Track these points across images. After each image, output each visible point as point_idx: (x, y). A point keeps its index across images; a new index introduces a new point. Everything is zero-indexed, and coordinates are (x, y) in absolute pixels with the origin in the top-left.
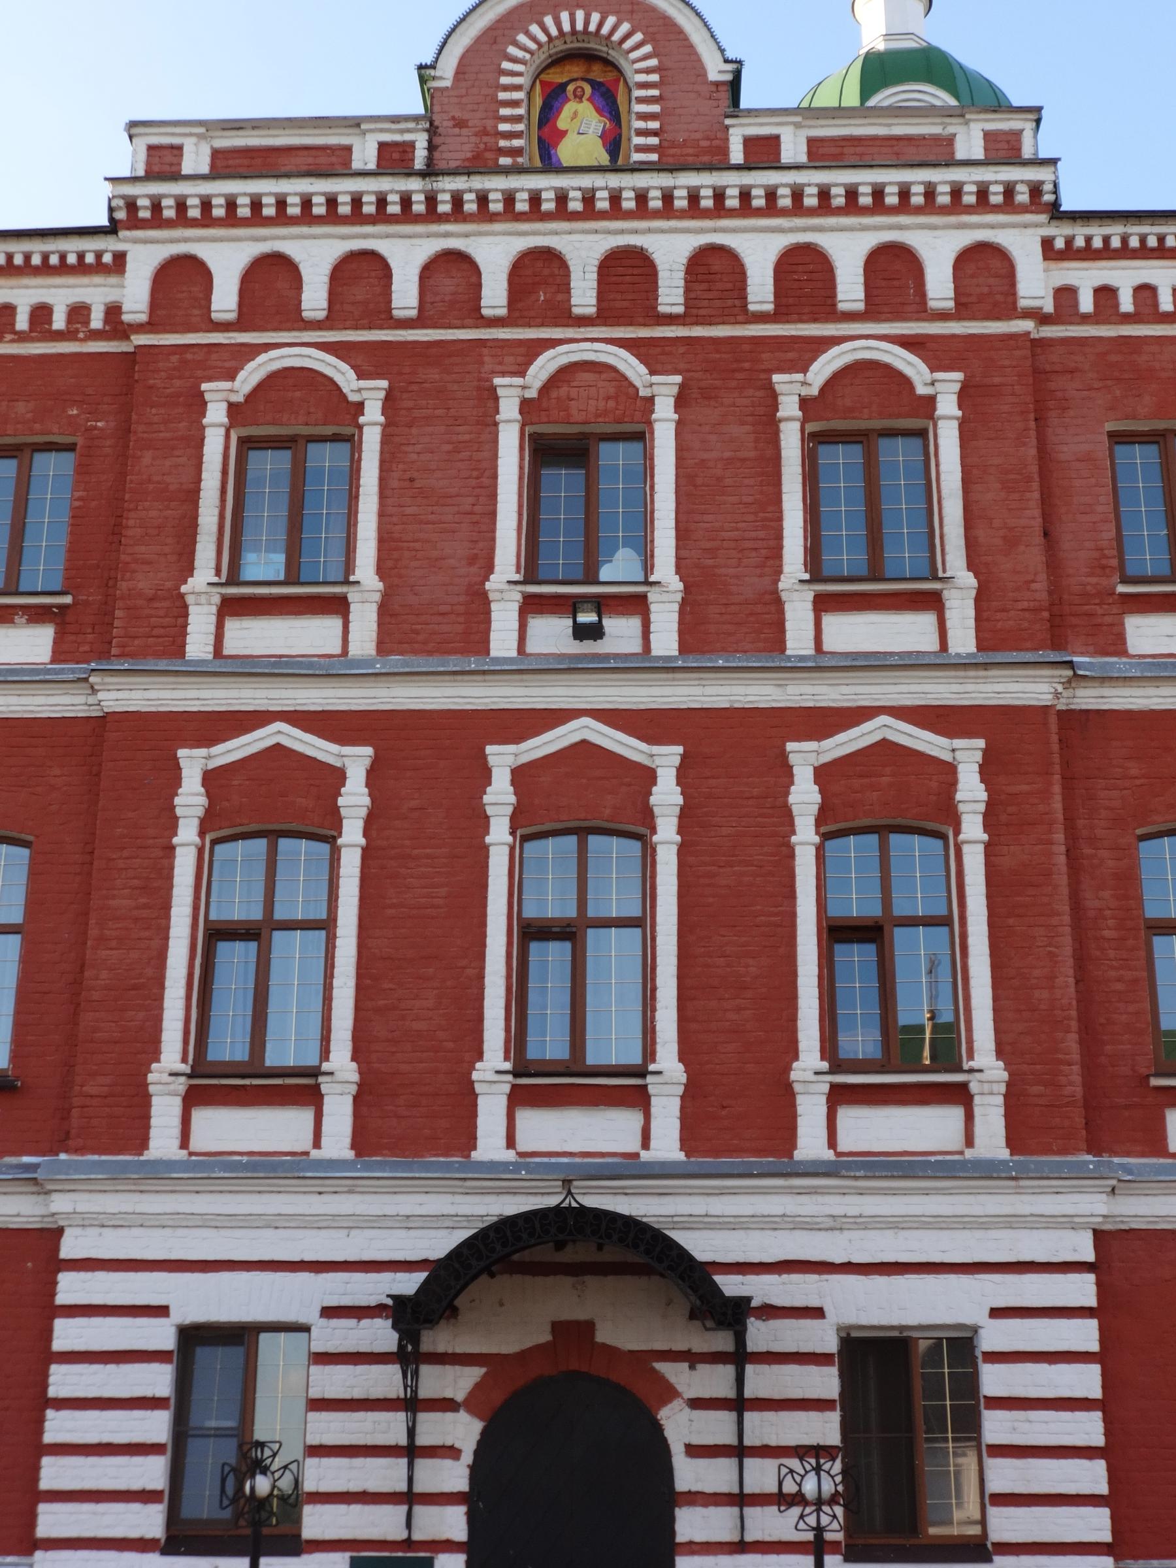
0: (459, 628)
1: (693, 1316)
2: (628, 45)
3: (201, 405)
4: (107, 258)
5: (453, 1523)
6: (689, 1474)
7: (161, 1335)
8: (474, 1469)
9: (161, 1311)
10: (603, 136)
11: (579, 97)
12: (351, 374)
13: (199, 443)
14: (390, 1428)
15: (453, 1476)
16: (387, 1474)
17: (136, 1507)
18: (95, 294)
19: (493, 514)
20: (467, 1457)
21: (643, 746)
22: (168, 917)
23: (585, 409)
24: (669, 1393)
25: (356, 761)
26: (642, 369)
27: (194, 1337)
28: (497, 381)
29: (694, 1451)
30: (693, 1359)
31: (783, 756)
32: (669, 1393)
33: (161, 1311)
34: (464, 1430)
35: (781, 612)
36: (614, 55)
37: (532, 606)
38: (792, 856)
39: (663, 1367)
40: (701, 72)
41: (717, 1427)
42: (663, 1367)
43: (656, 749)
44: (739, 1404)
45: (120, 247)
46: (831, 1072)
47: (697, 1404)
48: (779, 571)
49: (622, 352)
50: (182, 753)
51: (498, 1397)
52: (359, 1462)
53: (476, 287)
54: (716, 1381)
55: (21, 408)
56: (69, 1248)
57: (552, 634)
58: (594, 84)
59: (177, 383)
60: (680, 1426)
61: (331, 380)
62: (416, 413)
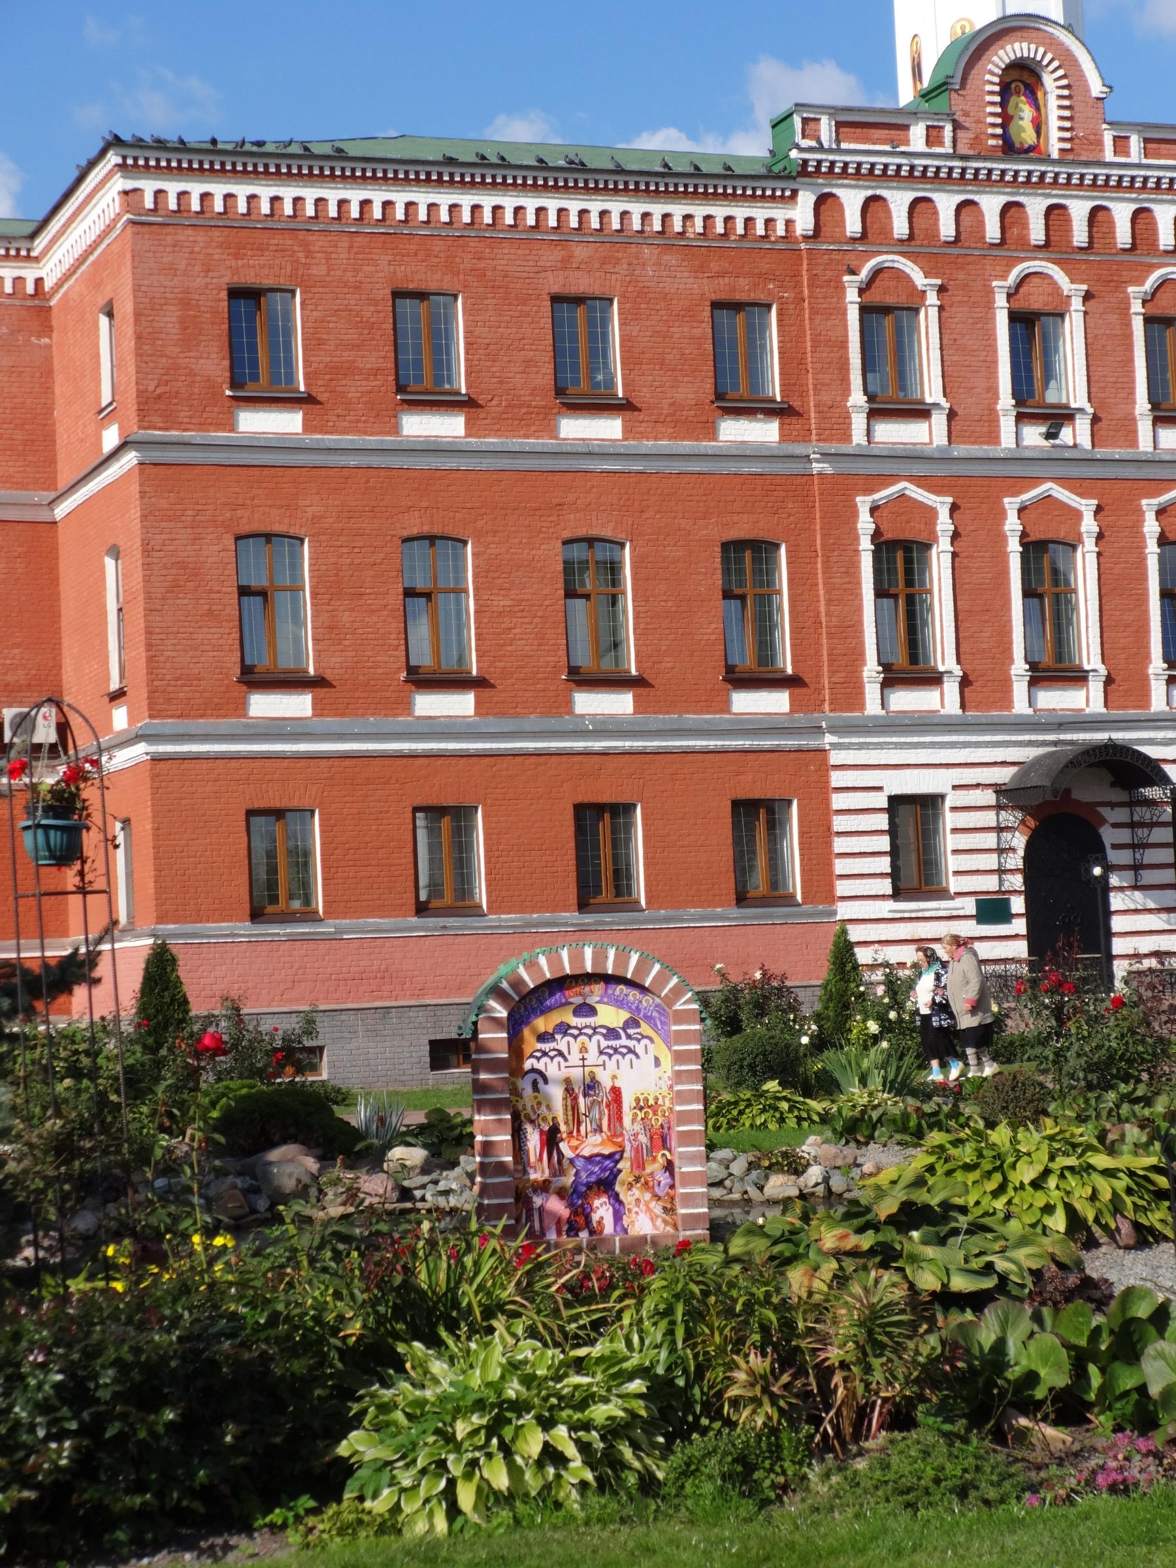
0: (986, 429)
1: (1113, 785)
2: (1051, 68)
3: (840, 289)
4: (788, 193)
5: (1017, 881)
6: (1114, 857)
7: (881, 801)
8: (1025, 858)
9: (880, 789)
10: (1032, 121)
11: (1018, 93)
12: (921, 274)
13: (844, 313)
14: (990, 840)
15: (1016, 861)
16: (991, 861)
17: (878, 880)
18: (780, 214)
19: (996, 362)
20: (1021, 852)
21: (1078, 499)
22: (860, 588)
23: (1035, 300)
24: (1103, 821)
25: (941, 504)
26: (1067, 279)
27: (897, 803)
28: (994, 283)
29: (1115, 847)
30: (1112, 805)
31: (1140, 506)
32: (1103, 821)
33: (880, 789)
34: (1019, 841)
35: (1136, 425)
36: (1038, 69)
37: (1020, 418)
38: (1145, 559)
39: (1102, 810)
40: (1087, 90)
41: (1124, 836)
42: (1102, 810)
43: (1084, 501)
44: (1132, 825)
45: (795, 186)
46: (1169, 669)
47: (1115, 825)
48: (1134, 402)
49: (1056, 268)
50: (858, 499)
51: (1032, 823)
52: (974, 856)
53: (981, 224)
54: (1121, 815)
55: (743, 282)
56: (835, 758)
57: (1033, 435)
58: (1027, 86)
59: (829, 273)
60: (1109, 835)
61: (908, 276)
62: (954, 299)
